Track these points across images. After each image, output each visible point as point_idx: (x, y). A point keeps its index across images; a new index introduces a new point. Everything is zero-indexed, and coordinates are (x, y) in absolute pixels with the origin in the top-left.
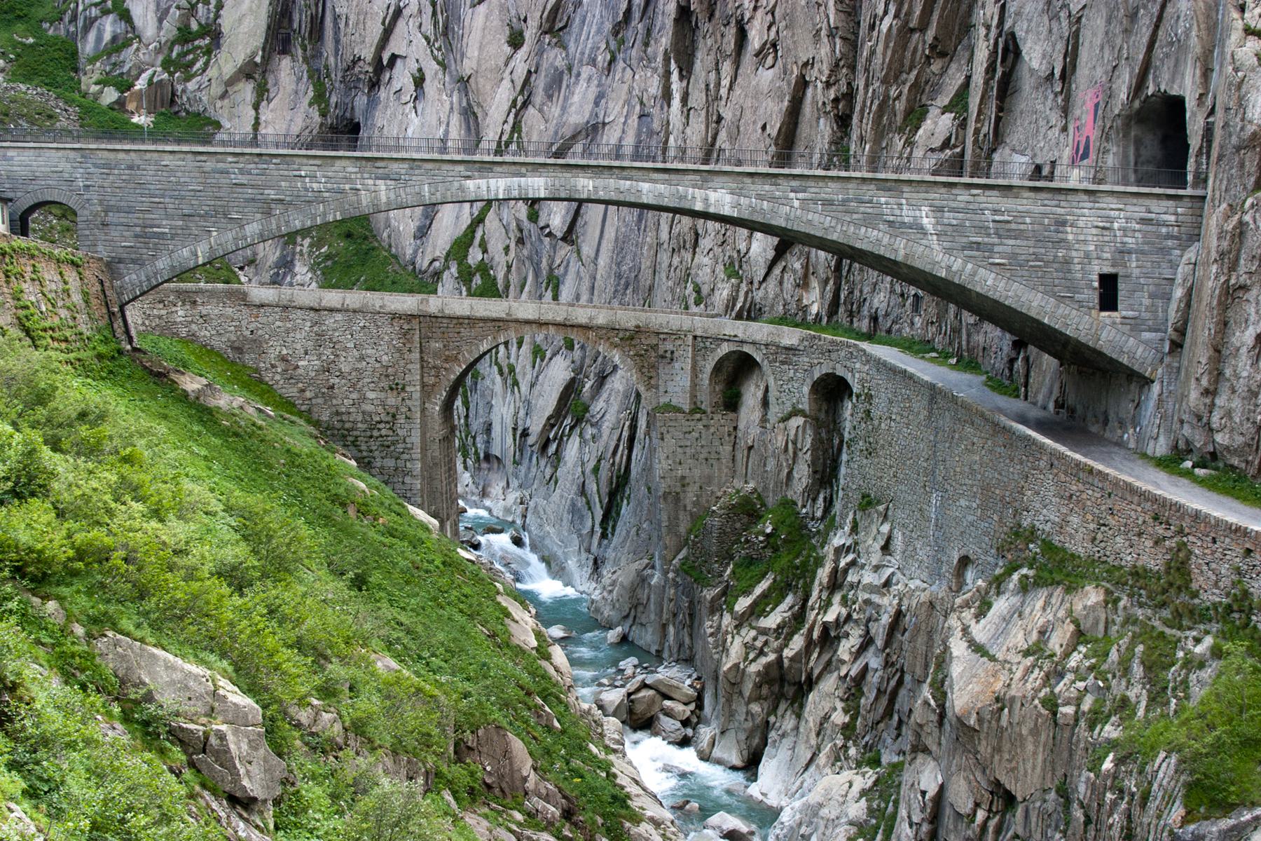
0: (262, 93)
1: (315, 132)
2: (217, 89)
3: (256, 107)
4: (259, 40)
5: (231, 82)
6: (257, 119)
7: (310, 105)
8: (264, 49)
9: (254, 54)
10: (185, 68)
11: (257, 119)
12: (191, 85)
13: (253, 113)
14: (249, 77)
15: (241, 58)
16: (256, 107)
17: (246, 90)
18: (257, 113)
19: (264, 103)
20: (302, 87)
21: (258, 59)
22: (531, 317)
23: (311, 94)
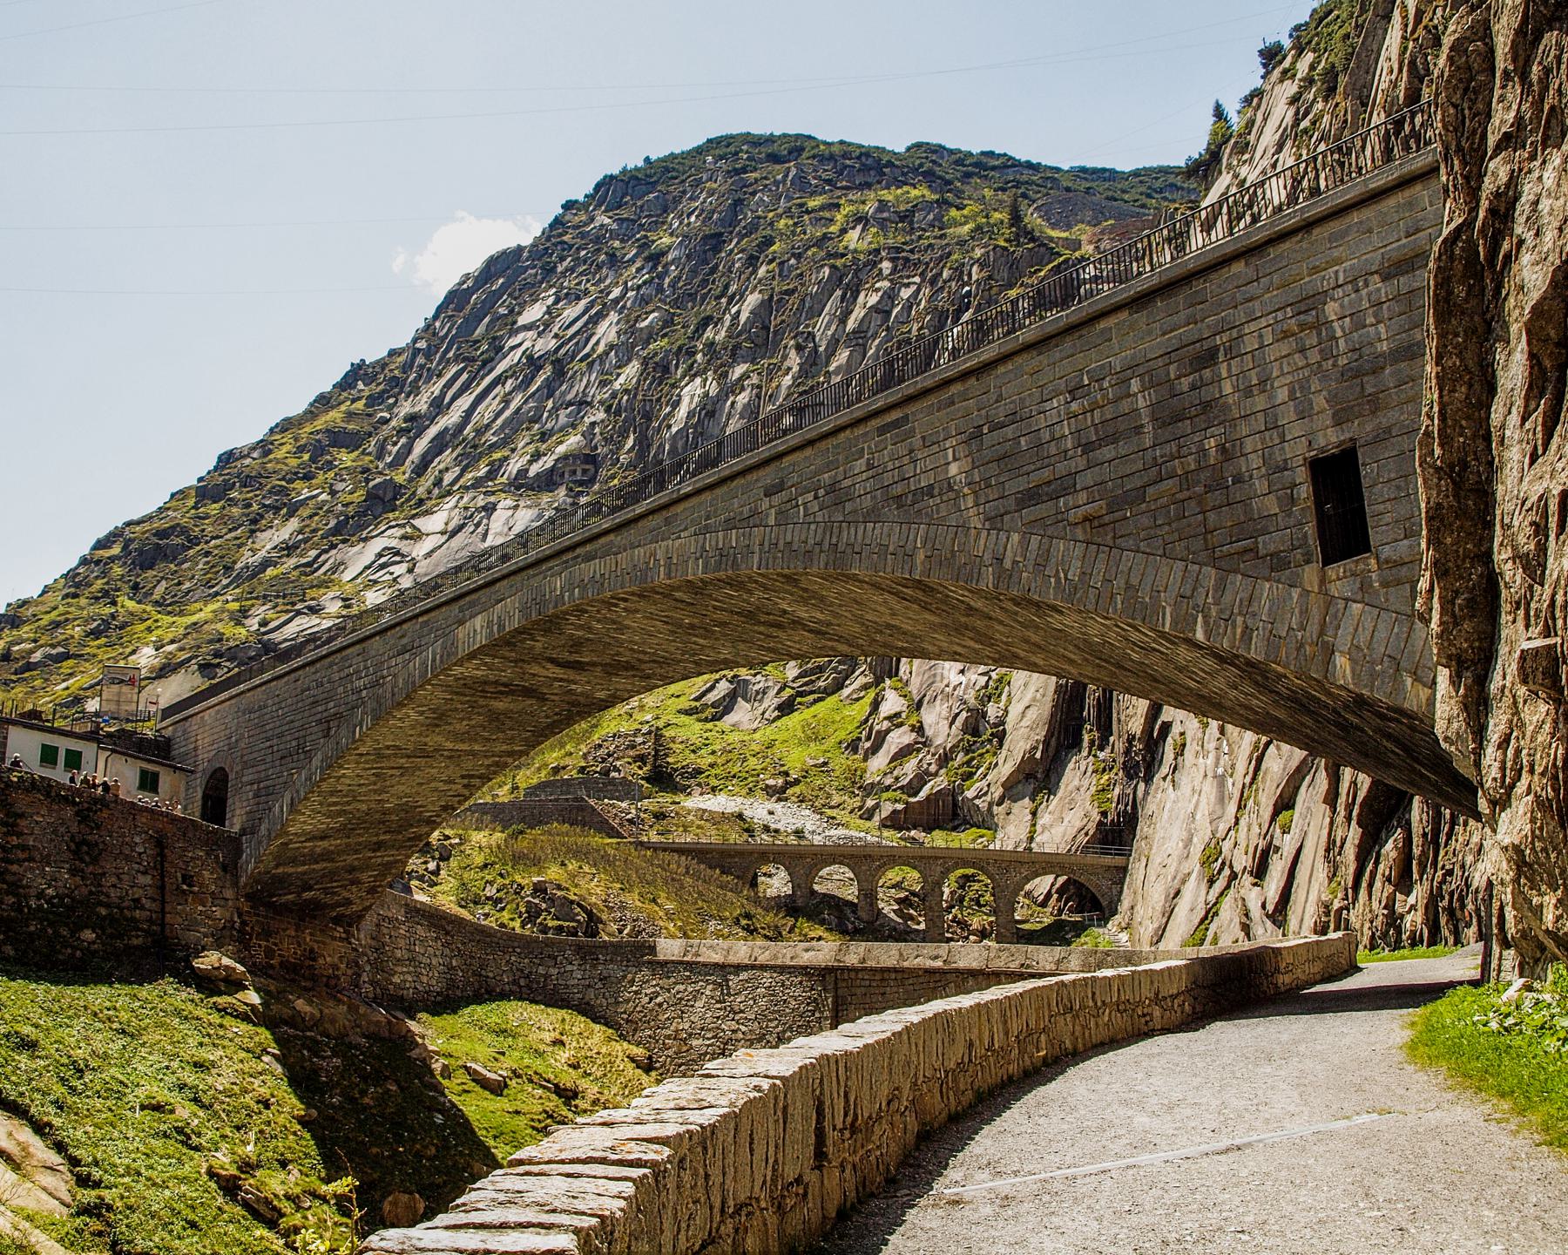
1: (1091, 833)
3: (1034, 814)
4: (1041, 734)
12: (970, 794)
13: (1030, 817)
22: (975, 965)
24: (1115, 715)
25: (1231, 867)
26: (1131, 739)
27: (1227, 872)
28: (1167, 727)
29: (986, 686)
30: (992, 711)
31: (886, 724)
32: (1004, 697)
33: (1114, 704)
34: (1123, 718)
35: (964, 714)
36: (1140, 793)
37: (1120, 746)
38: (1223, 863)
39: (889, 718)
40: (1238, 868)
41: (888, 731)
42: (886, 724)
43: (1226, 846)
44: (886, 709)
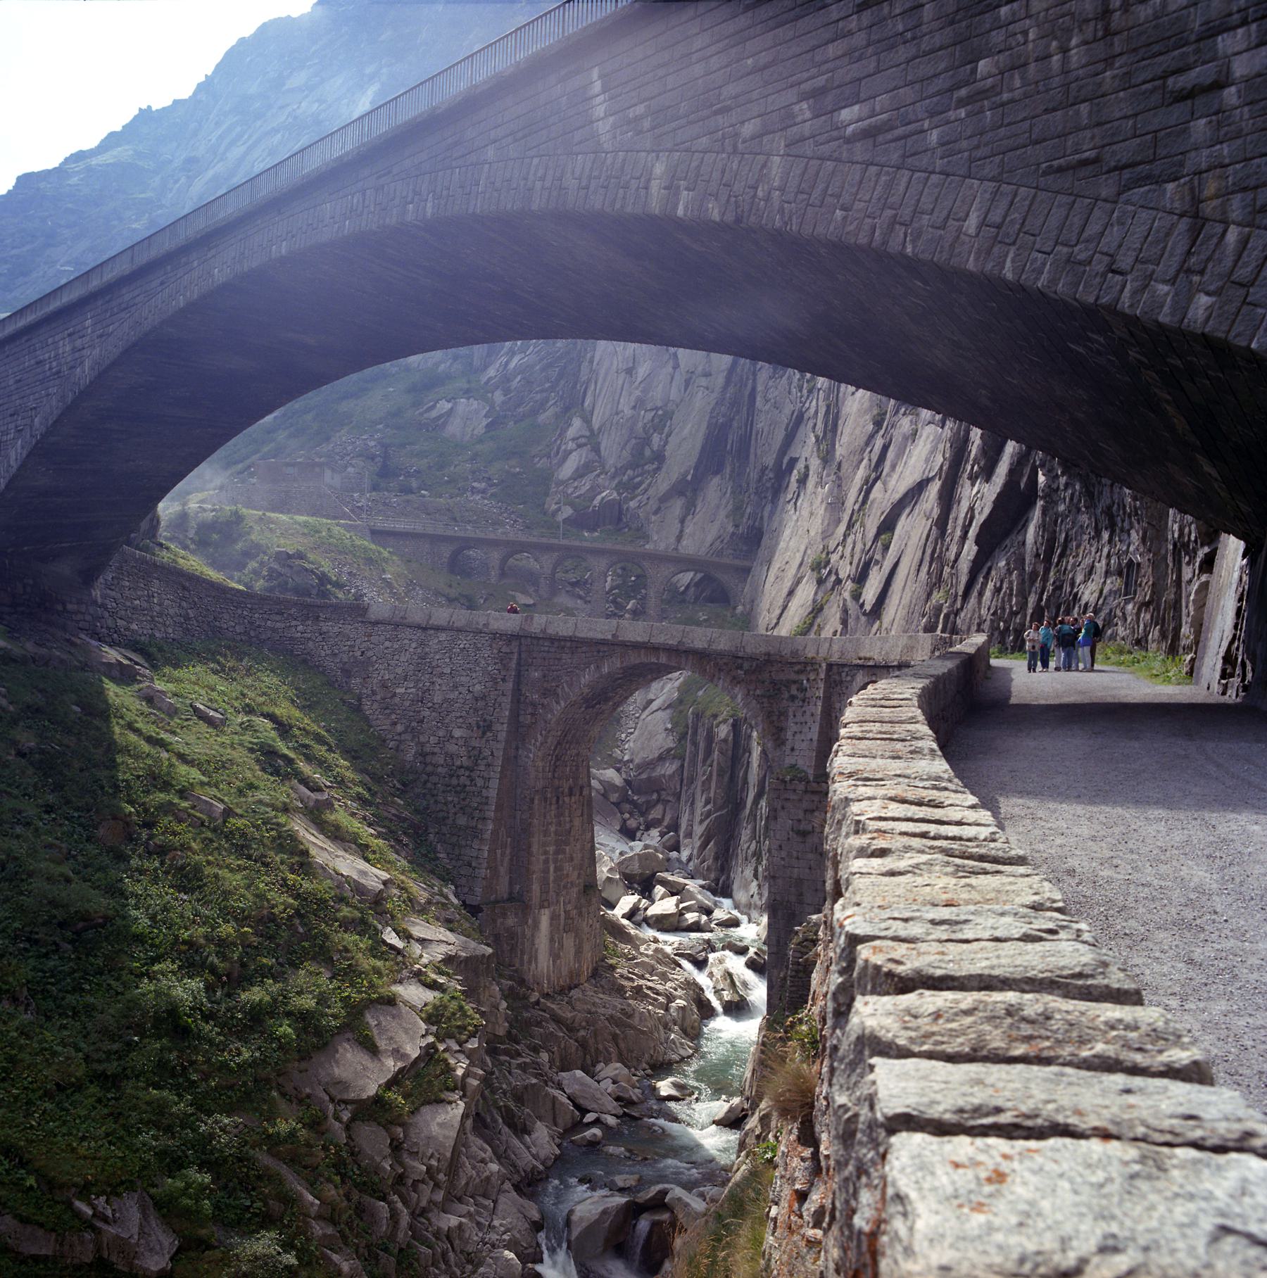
0: (690, 508)
2: (653, 504)
3: (682, 521)
4: (693, 460)
5: (664, 499)
6: (681, 531)
7: (727, 517)
8: (696, 468)
9: (687, 472)
10: (630, 488)
11: (681, 531)
12: (633, 504)
14: (681, 493)
15: (675, 476)
16: (682, 521)
17: (677, 506)
18: (682, 527)
19: (690, 517)
20: (724, 501)
21: (689, 478)
23: (730, 507)
24: (752, 450)
25: (837, 574)
26: (764, 469)
27: (833, 578)
28: (794, 461)
29: (652, 420)
30: (656, 439)
31: (571, 445)
32: (667, 429)
33: (753, 442)
34: (759, 452)
35: (634, 441)
36: (766, 514)
37: (754, 475)
38: (830, 572)
39: (573, 440)
40: (842, 575)
41: (571, 452)
42: (571, 445)
43: (834, 558)
44: (571, 433)
